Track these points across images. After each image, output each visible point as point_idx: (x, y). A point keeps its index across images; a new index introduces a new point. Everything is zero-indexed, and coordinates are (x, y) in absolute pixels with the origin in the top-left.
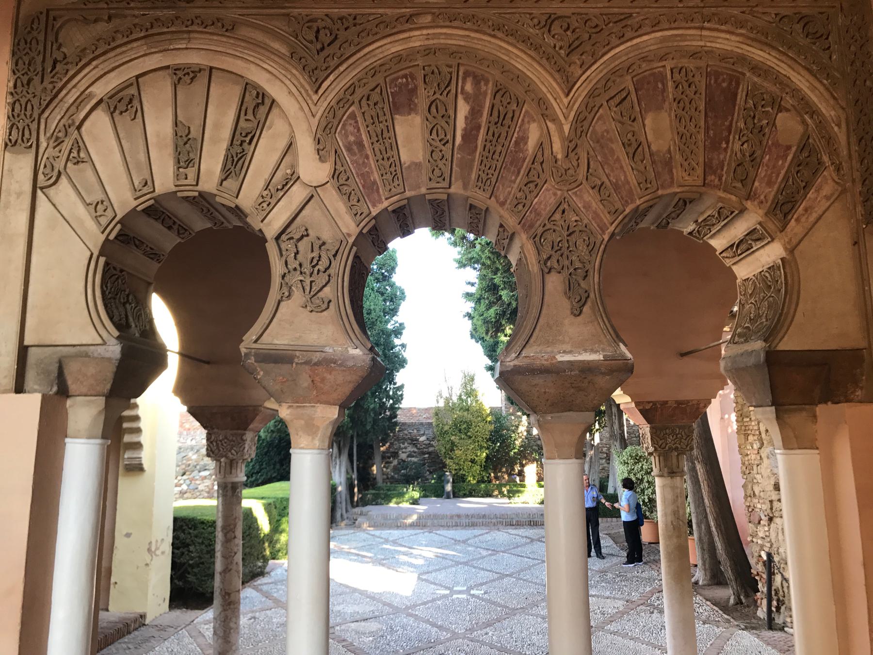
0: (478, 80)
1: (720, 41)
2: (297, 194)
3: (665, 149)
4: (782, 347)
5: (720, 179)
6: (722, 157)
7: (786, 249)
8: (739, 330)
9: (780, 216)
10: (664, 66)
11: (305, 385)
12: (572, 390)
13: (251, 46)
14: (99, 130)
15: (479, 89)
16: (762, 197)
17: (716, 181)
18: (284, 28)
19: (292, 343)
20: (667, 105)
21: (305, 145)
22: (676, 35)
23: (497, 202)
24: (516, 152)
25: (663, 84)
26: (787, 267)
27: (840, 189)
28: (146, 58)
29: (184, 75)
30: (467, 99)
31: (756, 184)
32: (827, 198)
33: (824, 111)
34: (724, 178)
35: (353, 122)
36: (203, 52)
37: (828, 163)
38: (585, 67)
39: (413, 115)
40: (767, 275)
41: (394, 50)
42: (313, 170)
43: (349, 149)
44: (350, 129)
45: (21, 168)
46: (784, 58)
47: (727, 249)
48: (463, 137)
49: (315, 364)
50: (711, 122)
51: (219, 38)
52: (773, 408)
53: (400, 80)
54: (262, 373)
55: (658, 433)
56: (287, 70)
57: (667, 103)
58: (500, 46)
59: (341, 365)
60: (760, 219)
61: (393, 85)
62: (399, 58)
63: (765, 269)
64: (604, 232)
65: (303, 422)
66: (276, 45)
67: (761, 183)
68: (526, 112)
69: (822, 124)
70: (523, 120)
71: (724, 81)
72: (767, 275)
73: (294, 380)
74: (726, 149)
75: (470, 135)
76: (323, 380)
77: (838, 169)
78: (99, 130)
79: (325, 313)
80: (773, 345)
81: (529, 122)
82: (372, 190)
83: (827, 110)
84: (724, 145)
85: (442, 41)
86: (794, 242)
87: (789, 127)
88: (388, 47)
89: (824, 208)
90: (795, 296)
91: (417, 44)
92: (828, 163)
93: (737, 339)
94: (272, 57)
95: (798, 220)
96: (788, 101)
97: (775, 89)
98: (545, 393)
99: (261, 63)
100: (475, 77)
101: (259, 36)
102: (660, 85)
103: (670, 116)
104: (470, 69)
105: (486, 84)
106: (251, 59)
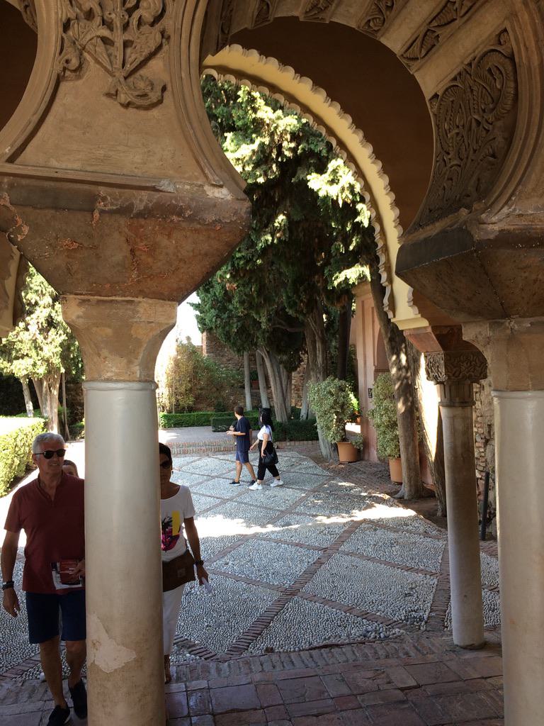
19: (89, 169)
54: (26, 230)
59: (191, 219)
73: (95, 247)
76: (153, 249)
79: (155, 112)
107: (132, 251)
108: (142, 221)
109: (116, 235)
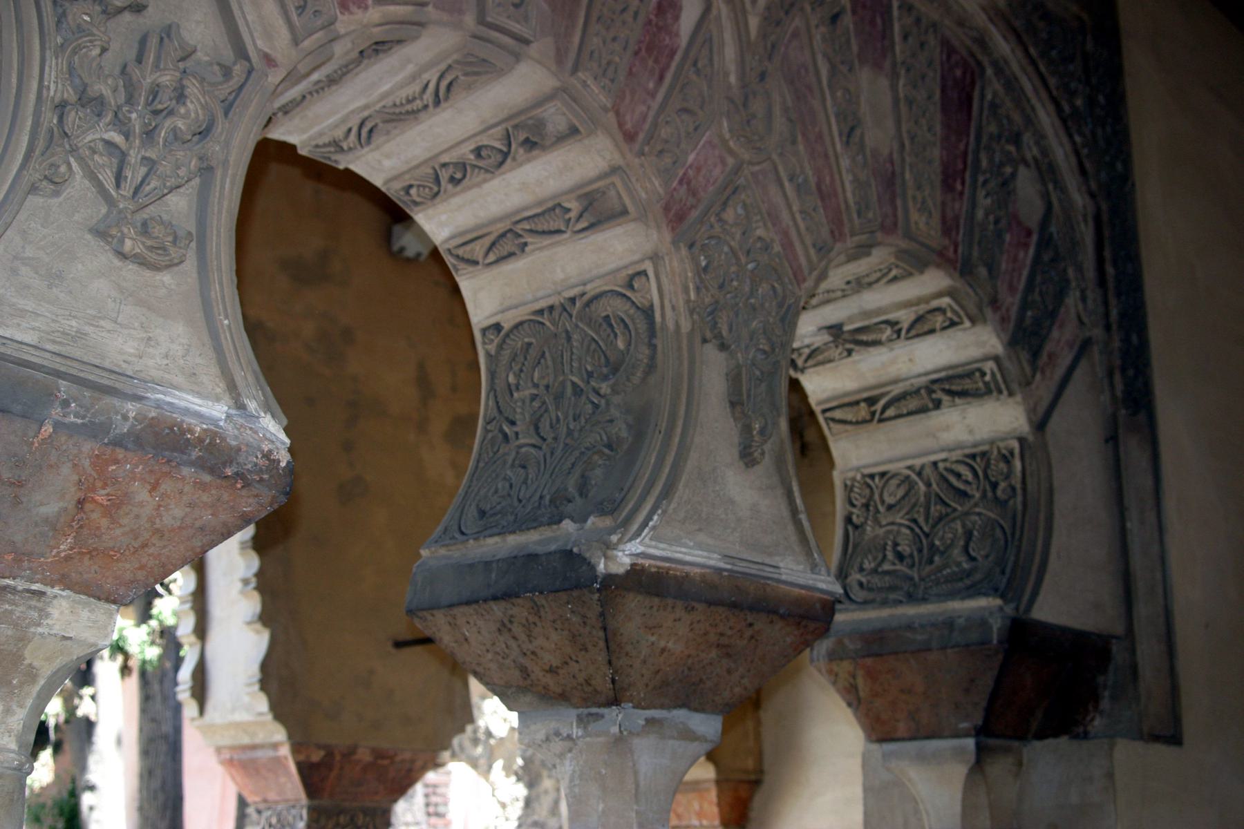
3: (886, 152)
5: (956, 251)
7: (1030, 421)
11: (51, 509)
12: (714, 653)
16: (1004, 309)
19: (49, 347)
20: (887, 64)
46: (1030, 69)
47: (857, 403)
49: (118, 442)
52: (970, 743)
73: (20, 484)
84: (959, 187)
86: (1041, 410)
98: (663, 650)
102: (879, 21)
107: (81, 503)
108: (120, 453)
109: (66, 470)
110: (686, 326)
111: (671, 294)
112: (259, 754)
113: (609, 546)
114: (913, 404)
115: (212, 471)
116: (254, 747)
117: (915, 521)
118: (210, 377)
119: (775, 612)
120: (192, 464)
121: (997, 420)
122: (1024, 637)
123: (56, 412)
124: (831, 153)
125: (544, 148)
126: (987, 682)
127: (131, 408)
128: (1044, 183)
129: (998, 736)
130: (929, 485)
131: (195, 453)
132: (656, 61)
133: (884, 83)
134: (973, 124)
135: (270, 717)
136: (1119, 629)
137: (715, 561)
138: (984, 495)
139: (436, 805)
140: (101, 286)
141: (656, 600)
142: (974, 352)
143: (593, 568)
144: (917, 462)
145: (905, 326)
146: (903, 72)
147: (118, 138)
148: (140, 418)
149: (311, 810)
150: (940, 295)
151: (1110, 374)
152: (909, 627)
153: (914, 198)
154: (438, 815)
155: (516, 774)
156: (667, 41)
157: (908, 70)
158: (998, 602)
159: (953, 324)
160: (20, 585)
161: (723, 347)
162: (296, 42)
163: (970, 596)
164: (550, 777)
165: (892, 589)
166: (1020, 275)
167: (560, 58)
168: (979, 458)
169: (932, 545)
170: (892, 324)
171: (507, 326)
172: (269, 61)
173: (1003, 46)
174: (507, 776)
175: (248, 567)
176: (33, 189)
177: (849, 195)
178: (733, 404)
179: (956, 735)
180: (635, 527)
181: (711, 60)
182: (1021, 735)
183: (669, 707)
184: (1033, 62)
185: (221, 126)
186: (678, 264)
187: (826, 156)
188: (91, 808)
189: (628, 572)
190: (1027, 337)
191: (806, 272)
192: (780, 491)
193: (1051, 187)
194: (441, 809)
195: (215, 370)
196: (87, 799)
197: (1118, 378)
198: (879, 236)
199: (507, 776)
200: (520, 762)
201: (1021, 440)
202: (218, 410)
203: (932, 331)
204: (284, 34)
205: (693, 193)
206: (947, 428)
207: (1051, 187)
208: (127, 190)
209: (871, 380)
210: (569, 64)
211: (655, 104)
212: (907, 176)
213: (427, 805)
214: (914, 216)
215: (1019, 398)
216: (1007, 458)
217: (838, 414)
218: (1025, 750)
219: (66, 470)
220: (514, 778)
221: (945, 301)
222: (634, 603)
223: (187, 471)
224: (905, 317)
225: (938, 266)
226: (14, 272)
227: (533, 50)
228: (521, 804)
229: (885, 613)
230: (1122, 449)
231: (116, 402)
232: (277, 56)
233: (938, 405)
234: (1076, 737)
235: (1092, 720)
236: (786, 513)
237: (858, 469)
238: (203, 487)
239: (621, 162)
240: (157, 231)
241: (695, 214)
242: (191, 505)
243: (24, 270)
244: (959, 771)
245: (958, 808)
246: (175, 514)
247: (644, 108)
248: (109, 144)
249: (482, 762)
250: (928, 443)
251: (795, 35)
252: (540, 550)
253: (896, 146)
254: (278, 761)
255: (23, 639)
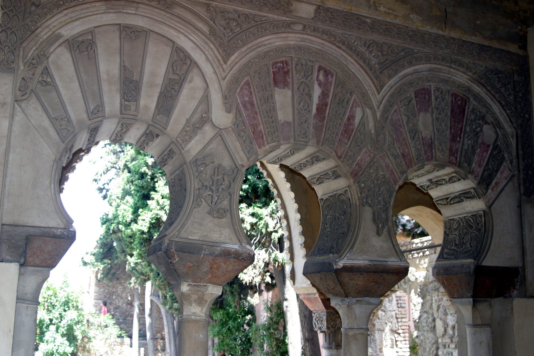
0: (327, 73)
1: (458, 76)
2: (208, 131)
3: (429, 137)
4: (485, 263)
5: (456, 160)
6: (457, 146)
7: (486, 205)
8: (446, 250)
9: (485, 186)
10: (430, 86)
11: (206, 269)
12: (372, 283)
13: (182, 22)
14: (62, 61)
15: (327, 80)
16: (476, 173)
17: (454, 161)
18: (203, 13)
19: (201, 239)
20: (430, 109)
21: (216, 99)
22: (437, 68)
23: (337, 155)
24: (348, 125)
25: (429, 95)
26: (486, 216)
27: (511, 174)
28: (103, 15)
29: (130, 34)
30: (320, 84)
31: (474, 165)
32: (506, 178)
33: (506, 128)
34: (458, 159)
35: (247, 87)
36: (146, 19)
37: (507, 159)
38: (390, 77)
39: (286, 89)
40: (471, 219)
41: (277, 44)
42: (221, 117)
43: (245, 106)
44: (246, 92)
45: (5, 84)
46: (489, 93)
47: (443, 199)
48: (317, 109)
49: (216, 256)
50: (452, 124)
51: (160, 11)
52: (471, 300)
53: (279, 64)
54: (177, 259)
55: (331, 316)
56: (206, 43)
57: (430, 108)
58: (342, 55)
60: (474, 186)
61: (274, 67)
62: (280, 50)
63: (469, 215)
64: (396, 184)
65: (197, 297)
66: (200, 25)
67: (476, 165)
68: (355, 99)
69: (505, 135)
70: (352, 105)
71: (459, 100)
72: (471, 219)
73: (198, 266)
74: (459, 142)
75: (321, 109)
77: (511, 163)
78: (62, 61)
80: (479, 262)
81: (356, 107)
82: (259, 136)
83: (509, 129)
84: (458, 139)
85: (308, 44)
86: (491, 202)
87: (488, 133)
88: (273, 41)
89: (504, 184)
90: (490, 234)
91: (292, 43)
92: (507, 159)
93: (445, 256)
94: (197, 32)
95: (492, 189)
96: (489, 118)
97: (484, 110)
98: (357, 284)
99: (188, 35)
100: (325, 71)
101: (188, 16)
102: (427, 97)
103: (432, 116)
104: (322, 64)
105: (332, 77)
106: (182, 31)
107: (211, 268)
108: (217, 258)
109: (207, 262)
110: (358, 203)
111: (355, 196)
112: (311, 296)
113: (336, 262)
114: (457, 200)
115: (237, 259)
116: (309, 294)
117: (460, 234)
118: (235, 240)
119: (389, 272)
120: (232, 258)
121: (476, 205)
122: (480, 272)
123: (204, 252)
124: (407, 143)
125: (320, 161)
126: (472, 283)
127: (219, 249)
128: (495, 128)
129: (481, 298)
130: (463, 223)
131: (233, 256)
132: (348, 134)
133: (429, 115)
134: (465, 118)
135: (311, 286)
136: (520, 265)
137: (367, 262)
138: (476, 228)
139: (401, 304)
140: (211, 224)
141: (351, 274)
142: (468, 186)
143: (333, 267)
144: (461, 216)
145: (447, 180)
146: (435, 110)
147: (211, 193)
148: (221, 250)
149: (327, 313)
150: (453, 173)
151: (519, 185)
152: (454, 267)
153: (438, 149)
154: (401, 307)
155: (418, 294)
156: (351, 127)
157: (437, 110)
158: (473, 261)
159: (459, 180)
160: (202, 284)
161: (370, 206)
162: (248, 160)
163: (468, 258)
164: (429, 295)
165: (453, 254)
166: (484, 160)
167: (318, 143)
168: (475, 216)
169: (463, 242)
170: (444, 180)
171: (324, 199)
172: (243, 166)
173: (477, 89)
174: (416, 295)
175: (302, 240)
176: (195, 208)
177: (414, 154)
178: (374, 221)
179: (467, 297)
180: (343, 257)
181: (365, 129)
182: (491, 297)
183: (363, 297)
184: (489, 91)
185: (232, 185)
186: (354, 187)
187: (406, 144)
188: (287, 307)
189: (342, 268)
190: (485, 181)
191: (398, 179)
192: (390, 241)
193: (498, 130)
194: (403, 305)
195: (236, 237)
196: (285, 303)
197: (522, 187)
198: (426, 163)
199: (416, 295)
200: (419, 290)
201: (484, 211)
202: (236, 247)
203: (455, 182)
204: (246, 159)
205: (360, 167)
206: (467, 207)
207: (498, 130)
208: (213, 204)
209: (446, 193)
210: (321, 143)
211: (347, 147)
212: (436, 142)
213: (398, 304)
214: (438, 154)
215: (482, 199)
216: (481, 216)
217: (439, 202)
218: (492, 301)
219: (207, 262)
220: (417, 296)
221: (454, 175)
222: (345, 274)
223: (231, 259)
224: (447, 178)
225: (449, 166)
226: (193, 225)
227: (310, 143)
228: (420, 305)
229: (449, 262)
230: (522, 209)
231: (216, 248)
232: (245, 164)
233: (463, 201)
234: (506, 297)
235: (513, 292)
236: (392, 246)
237: (447, 217)
238: (235, 262)
239: (337, 164)
240: (220, 211)
241: (360, 173)
242: (234, 266)
243: (195, 224)
244: (470, 308)
245: (471, 318)
246: (230, 268)
247: (344, 148)
248: (209, 195)
249: (408, 290)
250: (463, 211)
251: (395, 111)
252: (326, 261)
253: (432, 133)
254: (316, 298)
255: (204, 295)
